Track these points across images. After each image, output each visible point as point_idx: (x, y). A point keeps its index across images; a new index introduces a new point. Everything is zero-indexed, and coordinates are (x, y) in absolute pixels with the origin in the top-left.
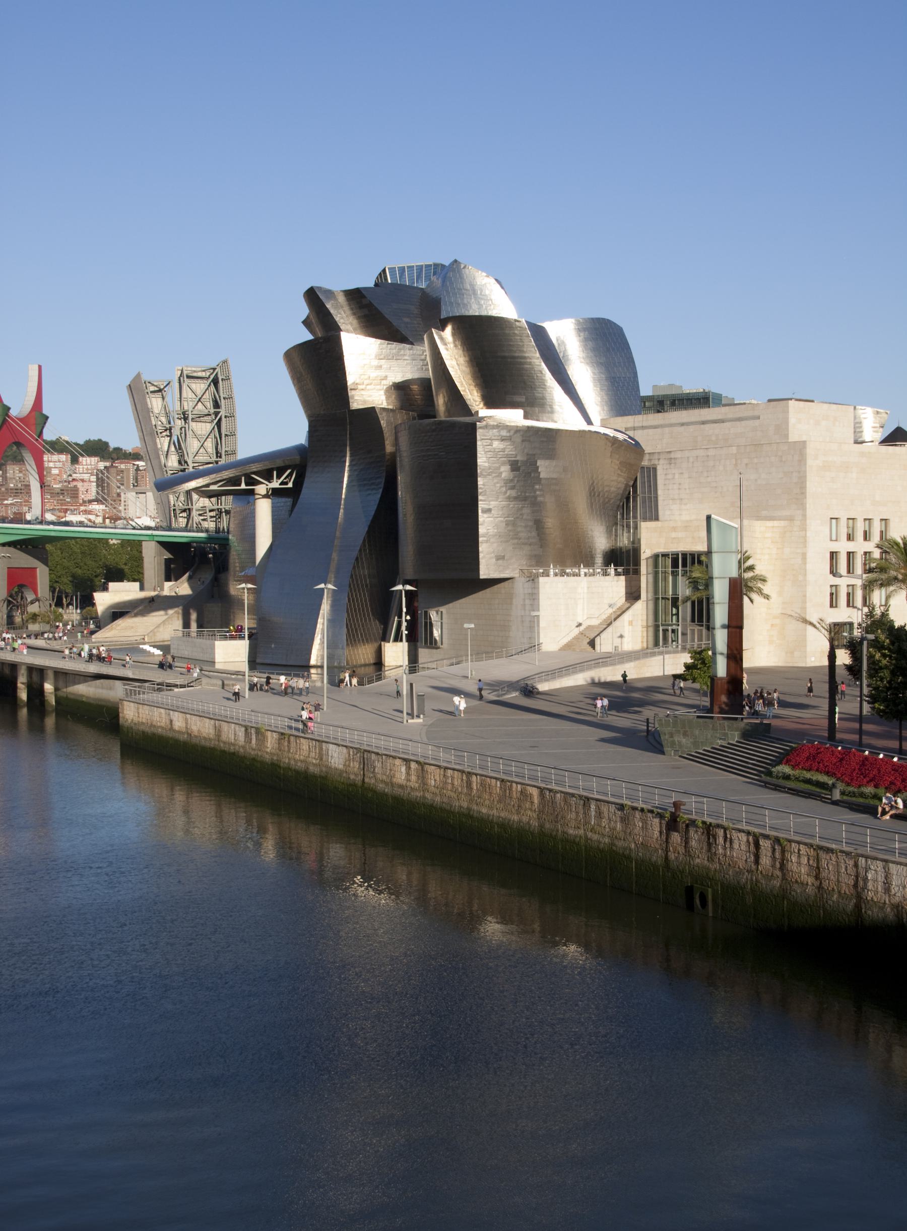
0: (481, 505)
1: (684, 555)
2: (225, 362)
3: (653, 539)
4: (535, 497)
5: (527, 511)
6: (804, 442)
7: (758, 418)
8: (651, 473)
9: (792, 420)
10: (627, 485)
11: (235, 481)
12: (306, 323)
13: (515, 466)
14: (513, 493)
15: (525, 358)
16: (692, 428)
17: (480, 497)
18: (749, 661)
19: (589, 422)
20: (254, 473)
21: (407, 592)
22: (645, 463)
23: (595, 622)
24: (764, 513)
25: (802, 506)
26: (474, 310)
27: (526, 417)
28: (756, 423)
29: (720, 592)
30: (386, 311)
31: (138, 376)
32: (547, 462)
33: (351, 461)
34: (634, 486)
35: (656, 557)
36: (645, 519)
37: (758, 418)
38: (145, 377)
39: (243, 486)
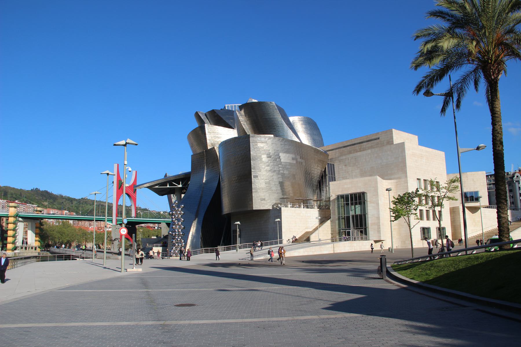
0: (253, 174)
1: (351, 195)
3: (336, 189)
5: (275, 177)
10: (321, 171)
13: (269, 156)
16: (348, 148)
17: (252, 170)
25: (405, 172)
28: (378, 141)
30: (224, 118)
32: (285, 154)
34: (325, 171)
35: (338, 196)
37: (379, 138)
39: (168, 186)
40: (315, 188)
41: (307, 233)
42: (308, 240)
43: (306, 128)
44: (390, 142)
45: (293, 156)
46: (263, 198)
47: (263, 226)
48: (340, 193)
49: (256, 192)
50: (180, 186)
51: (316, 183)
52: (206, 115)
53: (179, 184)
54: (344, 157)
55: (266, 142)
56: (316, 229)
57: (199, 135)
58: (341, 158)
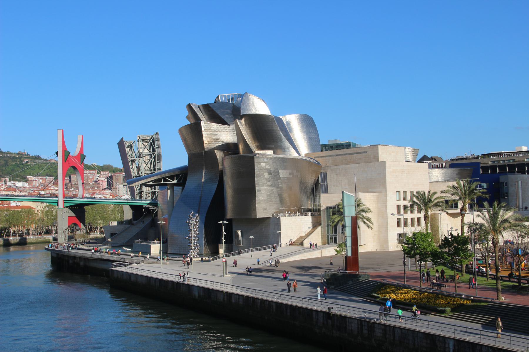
0: (257, 188)
2: (157, 133)
3: (326, 201)
4: (279, 185)
5: (275, 190)
6: (385, 162)
7: (367, 152)
8: (325, 175)
9: (380, 153)
11: (159, 180)
12: (188, 117)
13: (270, 173)
14: (269, 183)
15: (273, 130)
16: (340, 157)
18: (361, 250)
19: (300, 155)
20: (168, 177)
21: (225, 224)
22: (322, 171)
23: (304, 234)
24: (370, 190)
25: (385, 187)
26: (254, 112)
27: (274, 153)
28: (365, 154)
29: (348, 222)
30: (219, 112)
31: (122, 139)
32: (283, 171)
33: (205, 172)
35: (327, 208)
36: (323, 193)
38: (124, 140)
39: (162, 182)
40: (309, 195)
41: (301, 237)
42: (302, 244)
43: (302, 127)
44: (376, 158)
45: (290, 171)
46: (263, 208)
47: (265, 233)
48: (330, 205)
49: (259, 203)
50: (175, 181)
51: (309, 190)
52: (199, 107)
53: (173, 180)
54: (335, 167)
55: (267, 162)
56: (308, 235)
57: (193, 132)
58: (333, 167)
